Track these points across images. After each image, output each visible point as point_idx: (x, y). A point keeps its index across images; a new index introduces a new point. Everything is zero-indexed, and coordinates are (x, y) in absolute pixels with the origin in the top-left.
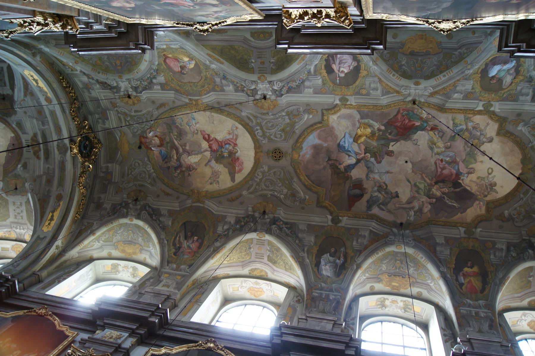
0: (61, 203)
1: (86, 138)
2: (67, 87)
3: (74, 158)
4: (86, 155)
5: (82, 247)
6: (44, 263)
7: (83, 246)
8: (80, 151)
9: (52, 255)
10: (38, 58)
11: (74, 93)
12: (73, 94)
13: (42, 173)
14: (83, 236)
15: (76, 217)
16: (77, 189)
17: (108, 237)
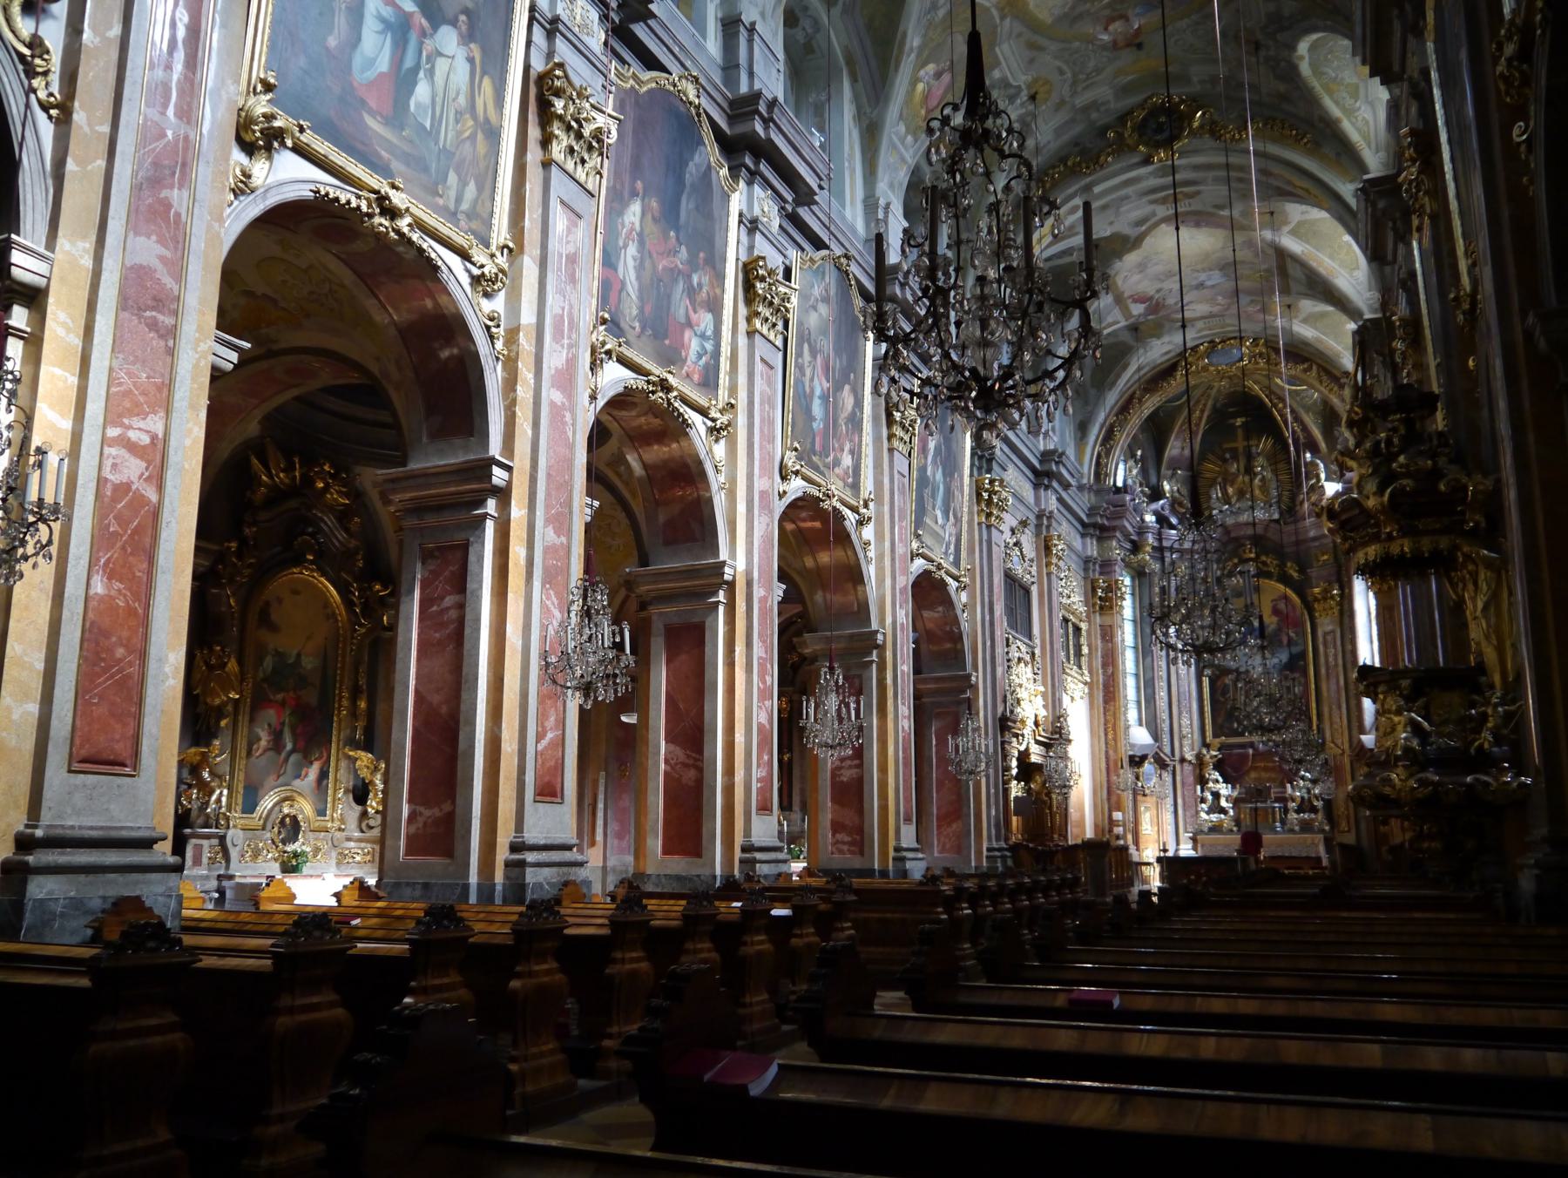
1: (1141, 128)
2: (1043, 187)
5: (1364, 145)
8: (1168, 143)
11: (1054, 167)
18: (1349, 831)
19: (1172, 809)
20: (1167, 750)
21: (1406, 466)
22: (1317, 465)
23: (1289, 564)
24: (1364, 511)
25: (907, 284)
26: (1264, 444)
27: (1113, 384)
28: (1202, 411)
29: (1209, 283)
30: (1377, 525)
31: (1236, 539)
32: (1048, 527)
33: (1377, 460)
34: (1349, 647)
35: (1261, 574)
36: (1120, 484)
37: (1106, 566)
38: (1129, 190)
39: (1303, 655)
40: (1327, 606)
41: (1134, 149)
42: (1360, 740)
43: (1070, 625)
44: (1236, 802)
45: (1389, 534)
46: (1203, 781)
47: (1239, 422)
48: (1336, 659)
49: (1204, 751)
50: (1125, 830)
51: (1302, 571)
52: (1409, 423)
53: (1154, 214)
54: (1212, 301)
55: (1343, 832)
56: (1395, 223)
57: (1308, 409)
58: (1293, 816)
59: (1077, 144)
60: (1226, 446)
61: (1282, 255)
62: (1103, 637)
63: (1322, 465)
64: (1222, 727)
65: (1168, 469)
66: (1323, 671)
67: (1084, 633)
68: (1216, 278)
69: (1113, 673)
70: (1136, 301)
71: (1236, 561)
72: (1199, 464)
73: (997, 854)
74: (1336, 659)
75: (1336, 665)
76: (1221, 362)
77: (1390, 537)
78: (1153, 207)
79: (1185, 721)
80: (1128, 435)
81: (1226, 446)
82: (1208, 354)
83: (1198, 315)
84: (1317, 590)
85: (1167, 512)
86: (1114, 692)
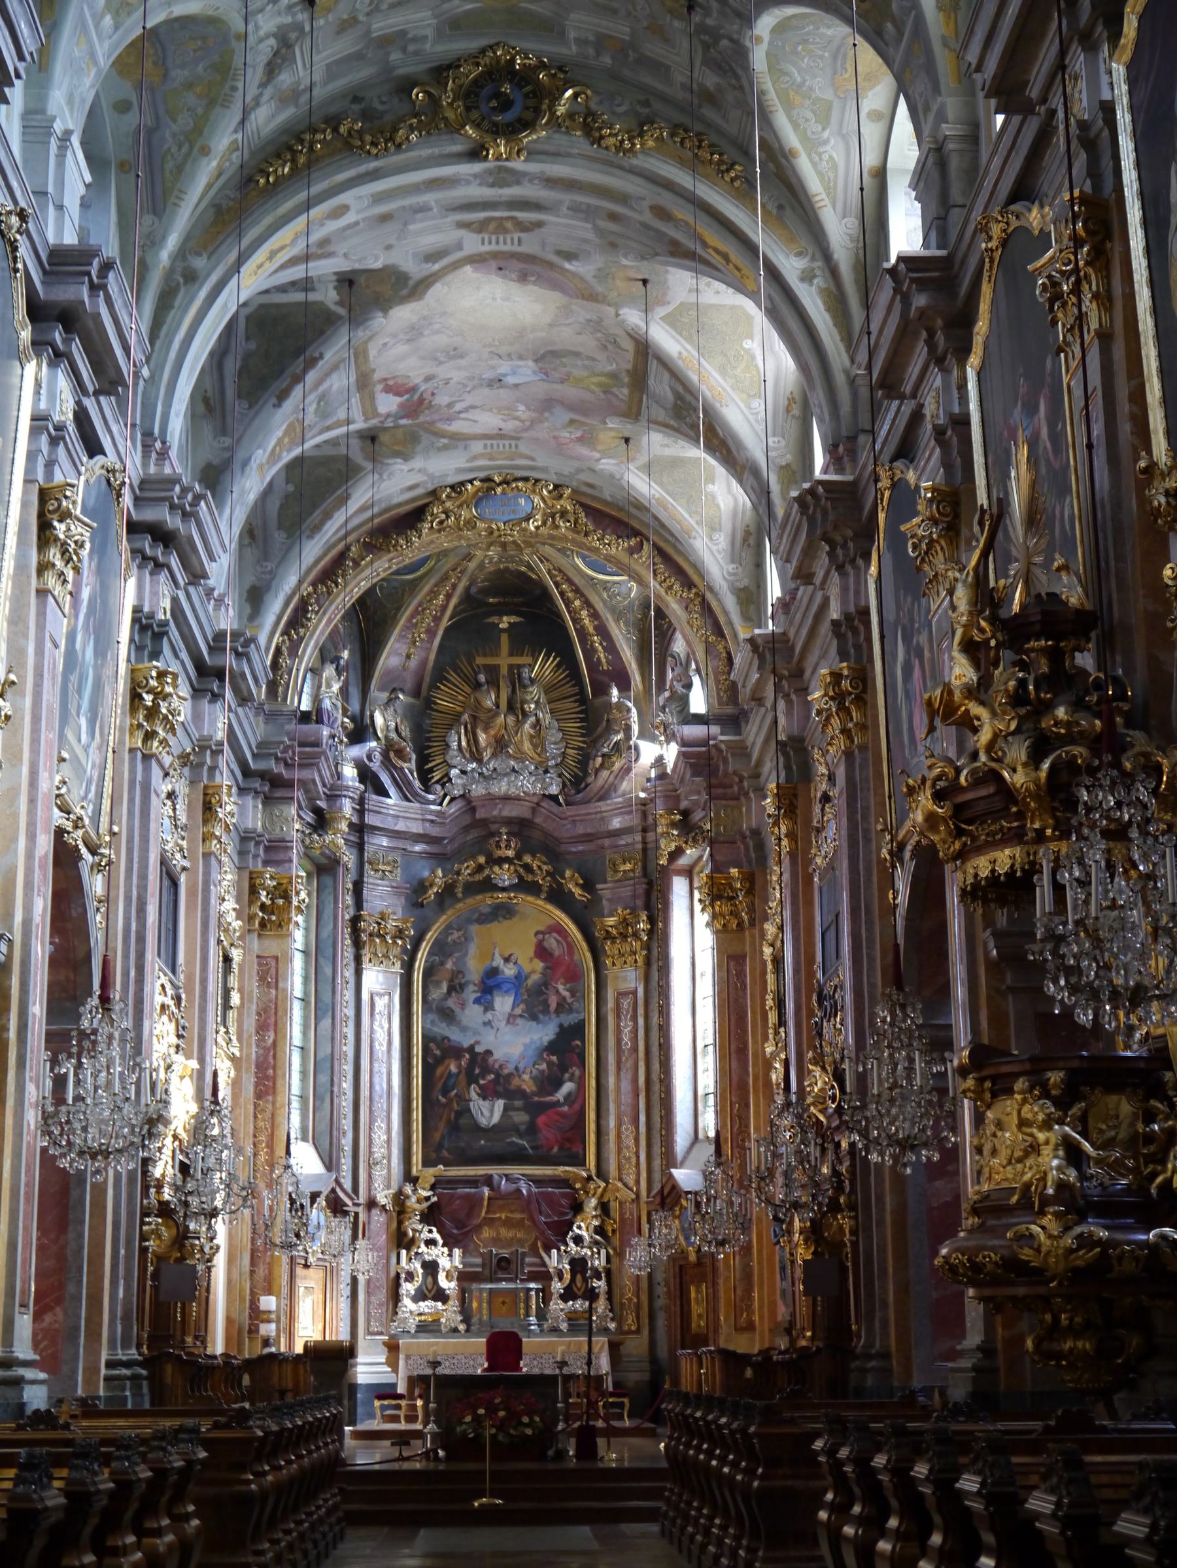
0: (680, 216)
2: (293, 161)
3: (533, 154)
4: (531, 102)
5: (827, 202)
6: (838, 338)
7: (824, 196)
8: (511, 131)
9: (825, 303)
10: (199, 263)
11: (314, 131)
12: (319, 136)
13: (590, 226)
14: (793, 180)
15: (733, 180)
16: (639, 161)
17: (813, 112)
18: (638, 1331)
19: (347, 1291)
20: (347, 1185)
21: (1068, 725)
22: (629, 710)
23: (568, 873)
24: (1007, 792)
25: (104, 287)
26: (543, 667)
27: (317, 528)
28: (449, 597)
29: (511, 380)
30: (1020, 816)
31: (485, 822)
32: (213, 769)
33: (1022, 711)
34: (655, 1020)
35: (525, 886)
36: (305, 706)
37: (276, 849)
38: (430, 198)
39: (578, 1030)
40: (626, 948)
41: (455, 129)
42: (671, 1176)
44: (465, 1278)
45: (1040, 833)
46: (402, 1241)
47: (505, 622)
48: (635, 1039)
49: (408, 1189)
50: (278, 1330)
51: (588, 886)
52: (1056, 656)
53: (459, 246)
54: (508, 411)
55: (630, 1332)
56: (931, 334)
57: (618, 615)
58: (557, 1306)
59: (356, 99)
60: (480, 661)
61: (644, 350)
62: (262, 978)
63: (634, 710)
64: (440, 1146)
65: (382, 689)
66: (611, 1058)
67: (235, 966)
68: (526, 372)
69: (275, 1043)
70: (388, 390)
71: (482, 860)
72: (433, 686)
73: (125, 1372)
74: (635, 1039)
75: (635, 1049)
76: (497, 515)
77: (1040, 837)
78: (462, 232)
79: (380, 1136)
80: (330, 621)
81: (480, 661)
82: (478, 501)
83: (478, 430)
84: (611, 921)
85: (376, 766)
86: (274, 1080)
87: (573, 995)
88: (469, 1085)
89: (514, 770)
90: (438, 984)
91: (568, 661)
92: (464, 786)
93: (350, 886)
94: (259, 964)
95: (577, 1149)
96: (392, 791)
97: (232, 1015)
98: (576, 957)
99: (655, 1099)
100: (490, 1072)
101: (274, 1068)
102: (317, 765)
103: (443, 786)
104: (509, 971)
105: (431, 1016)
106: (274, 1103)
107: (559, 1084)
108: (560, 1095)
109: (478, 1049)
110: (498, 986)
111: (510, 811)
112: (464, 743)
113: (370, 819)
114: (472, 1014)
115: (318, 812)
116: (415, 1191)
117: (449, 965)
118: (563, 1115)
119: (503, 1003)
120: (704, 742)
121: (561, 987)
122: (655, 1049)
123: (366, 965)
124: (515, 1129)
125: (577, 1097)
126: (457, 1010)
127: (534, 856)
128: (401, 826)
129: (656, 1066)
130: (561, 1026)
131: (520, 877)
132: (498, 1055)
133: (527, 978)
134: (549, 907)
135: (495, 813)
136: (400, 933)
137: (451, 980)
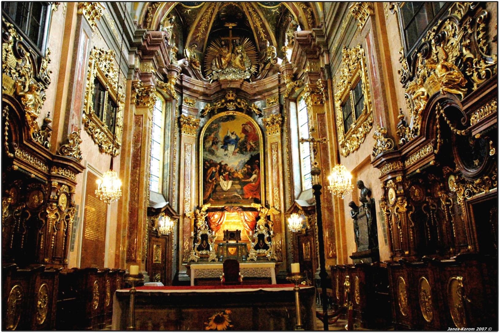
20: (175, 209)
23: (253, 105)
35: (238, 109)
43: (106, 92)
48: (277, 158)
49: (198, 211)
60: (222, 38)
63: (275, 48)
69: (141, 147)
71: (223, 101)
74: (277, 158)
75: (278, 162)
79: (188, 193)
87: (256, 145)
88: (220, 176)
89: (234, 71)
90: (209, 142)
91: (252, 39)
92: (217, 76)
93: (177, 106)
94: (136, 118)
95: (258, 197)
96: (193, 77)
97: (118, 130)
98: (256, 133)
99: (287, 178)
100: (227, 171)
101: (140, 157)
102: (159, 45)
103: (210, 76)
104: (233, 137)
105: (206, 153)
106: (140, 170)
107: (251, 175)
108: (252, 179)
109: (223, 164)
110: (230, 142)
111: (232, 86)
112: (217, 64)
113: (184, 83)
114: (220, 152)
115: (164, 75)
116: (200, 212)
117: (212, 135)
118: (253, 186)
119: (231, 148)
120: (305, 36)
121: (251, 143)
122: (286, 162)
123: (183, 134)
124: (236, 191)
125: (258, 180)
126: (215, 150)
127: (241, 100)
128: (195, 88)
129: (286, 167)
130: (251, 155)
131: (237, 107)
132: (230, 165)
133: (239, 139)
134: (247, 116)
135: (228, 86)
136: (195, 124)
137: (213, 141)
